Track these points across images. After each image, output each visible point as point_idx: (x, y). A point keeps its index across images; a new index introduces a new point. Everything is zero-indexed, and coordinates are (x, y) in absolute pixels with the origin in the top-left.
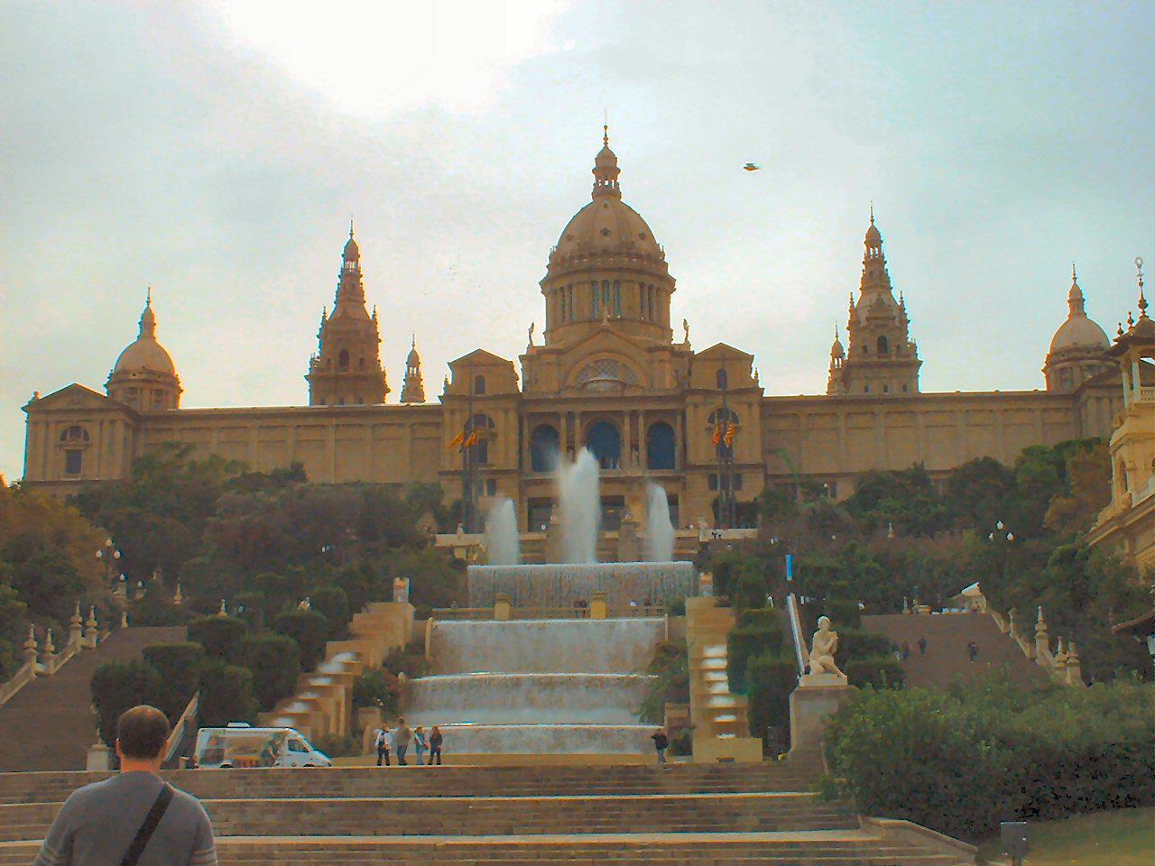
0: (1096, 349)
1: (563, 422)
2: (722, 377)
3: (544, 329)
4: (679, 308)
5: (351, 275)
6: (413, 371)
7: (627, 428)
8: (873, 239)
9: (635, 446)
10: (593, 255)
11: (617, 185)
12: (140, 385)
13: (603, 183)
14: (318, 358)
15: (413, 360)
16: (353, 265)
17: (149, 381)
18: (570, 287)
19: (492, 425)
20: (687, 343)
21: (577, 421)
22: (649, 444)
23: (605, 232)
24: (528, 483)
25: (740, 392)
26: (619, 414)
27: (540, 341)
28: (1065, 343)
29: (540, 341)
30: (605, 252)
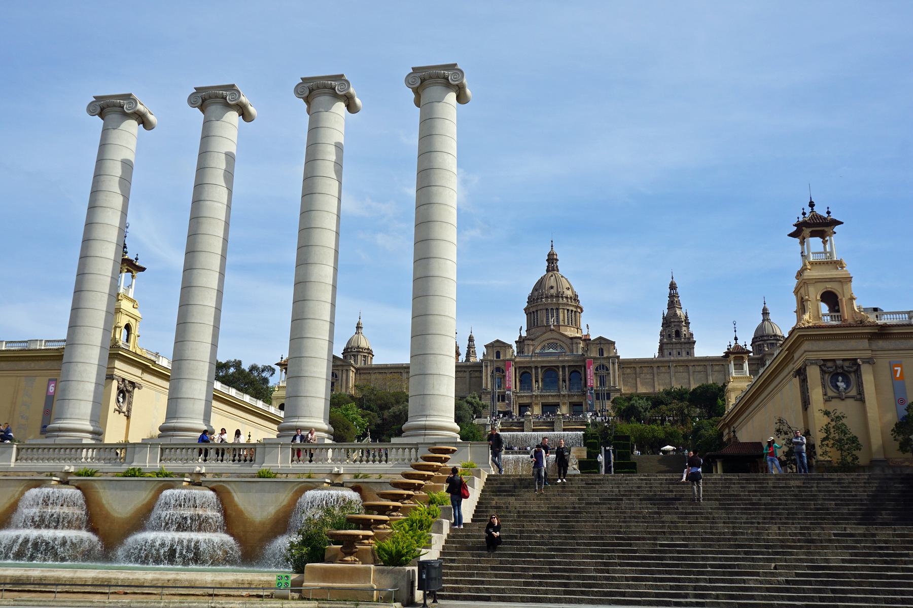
0: (775, 335)
2: (601, 352)
4: (584, 319)
8: (673, 286)
9: (564, 381)
10: (547, 297)
19: (503, 372)
20: (588, 335)
22: (570, 380)
23: (552, 287)
24: (519, 397)
25: (608, 358)
26: (557, 367)
27: (524, 334)
28: (760, 333)
29: (524, 334)
30: (552, 296)
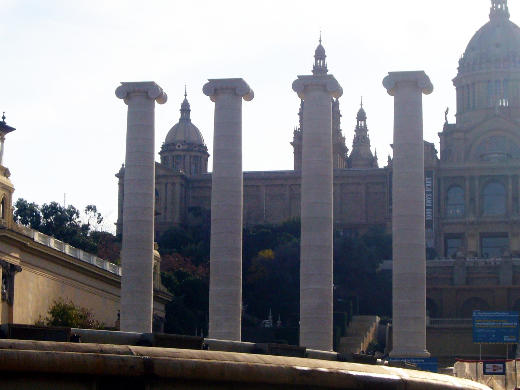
1: (467, 184)
3: (455, 113)
5: (320, 70)
6: (361, 124)
7: (510, 187)
11: (507, 8)
12: (182, 153)
13: (497, 7)
14: (299, 129)
15: (361, 116)
16: (320, 63)
17: (187, 150)
18: (473, 84)
21: (477, 183)
23: (498, 45)
27: (452, 120)
29: (452, 120)
